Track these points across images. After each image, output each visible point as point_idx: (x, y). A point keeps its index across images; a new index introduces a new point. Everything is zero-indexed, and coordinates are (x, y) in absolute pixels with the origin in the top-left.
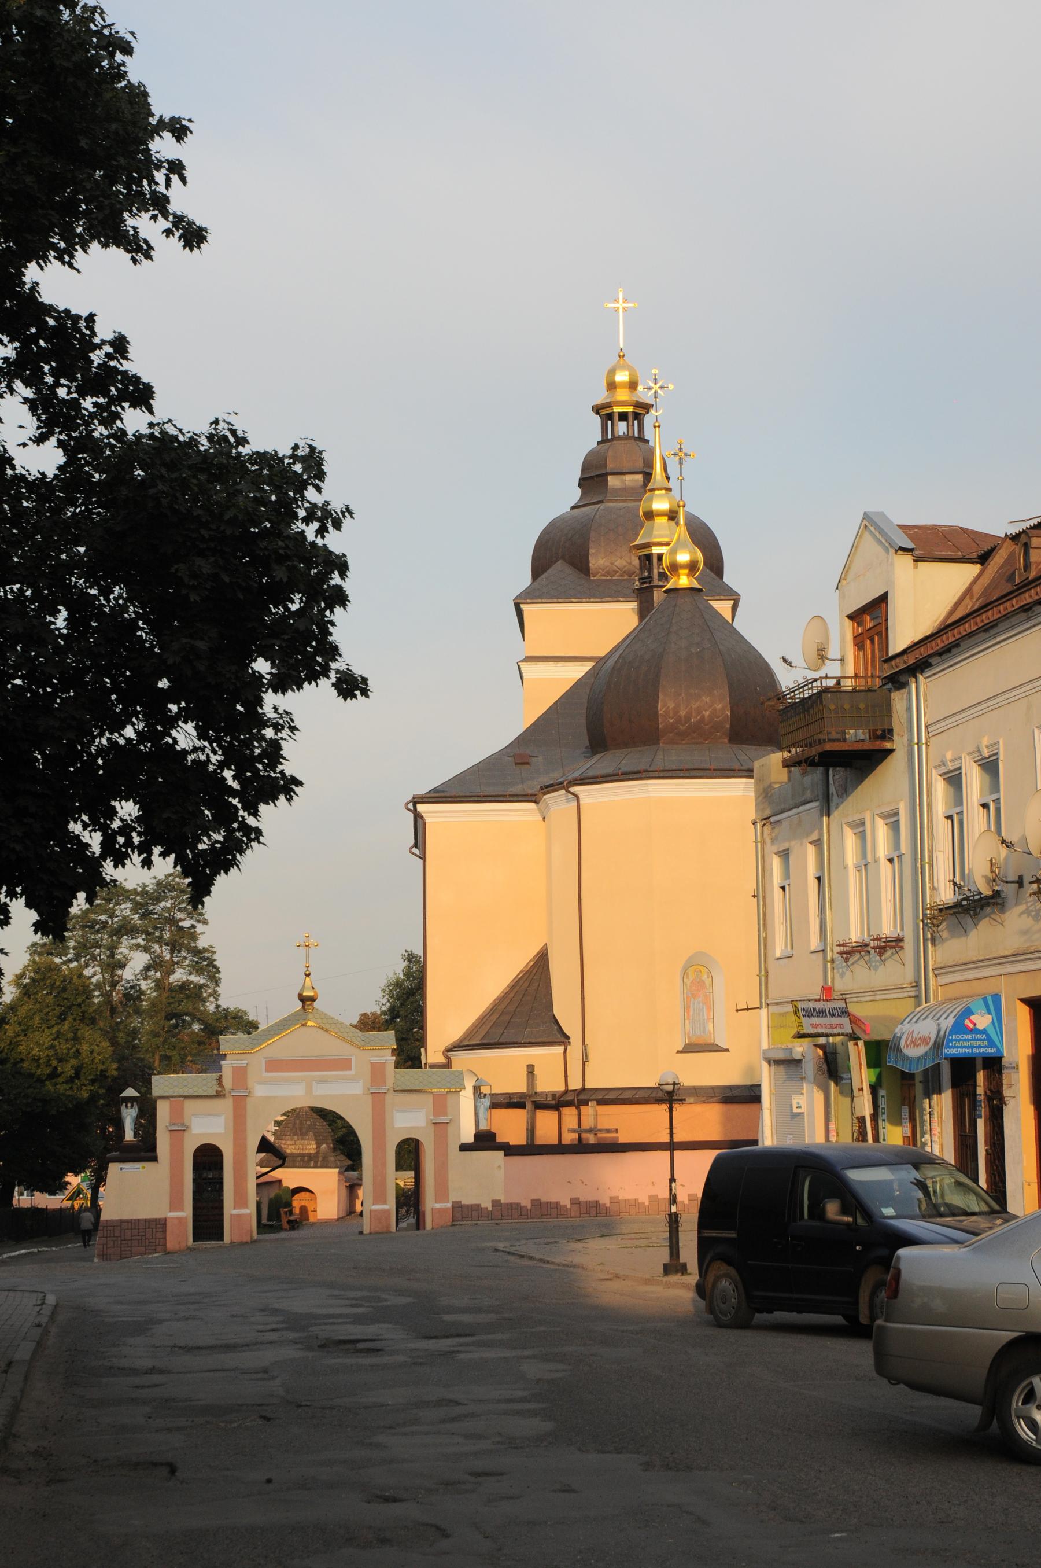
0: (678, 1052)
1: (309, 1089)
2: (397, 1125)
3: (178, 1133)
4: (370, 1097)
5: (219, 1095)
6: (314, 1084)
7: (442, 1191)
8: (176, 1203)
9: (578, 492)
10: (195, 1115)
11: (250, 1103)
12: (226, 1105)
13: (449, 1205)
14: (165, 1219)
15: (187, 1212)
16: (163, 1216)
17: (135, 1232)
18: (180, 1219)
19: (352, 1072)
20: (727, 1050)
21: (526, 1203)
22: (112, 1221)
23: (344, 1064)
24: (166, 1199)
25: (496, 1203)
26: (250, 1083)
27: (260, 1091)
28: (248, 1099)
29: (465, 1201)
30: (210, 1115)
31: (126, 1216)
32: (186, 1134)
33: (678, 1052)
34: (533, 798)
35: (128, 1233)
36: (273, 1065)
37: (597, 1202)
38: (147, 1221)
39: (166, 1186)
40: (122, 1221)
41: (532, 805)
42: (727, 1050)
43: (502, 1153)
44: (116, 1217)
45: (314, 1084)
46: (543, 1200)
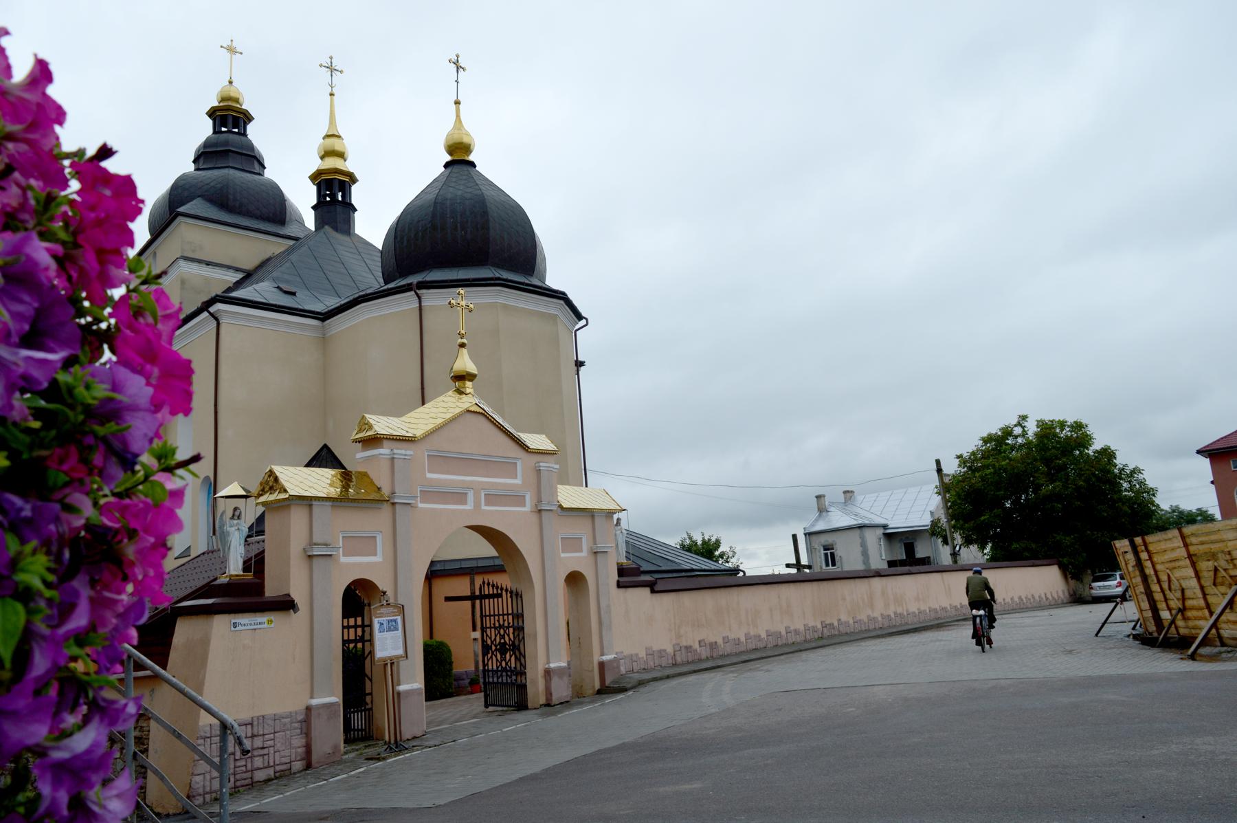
9: (191, 168)
23: (508, 467)
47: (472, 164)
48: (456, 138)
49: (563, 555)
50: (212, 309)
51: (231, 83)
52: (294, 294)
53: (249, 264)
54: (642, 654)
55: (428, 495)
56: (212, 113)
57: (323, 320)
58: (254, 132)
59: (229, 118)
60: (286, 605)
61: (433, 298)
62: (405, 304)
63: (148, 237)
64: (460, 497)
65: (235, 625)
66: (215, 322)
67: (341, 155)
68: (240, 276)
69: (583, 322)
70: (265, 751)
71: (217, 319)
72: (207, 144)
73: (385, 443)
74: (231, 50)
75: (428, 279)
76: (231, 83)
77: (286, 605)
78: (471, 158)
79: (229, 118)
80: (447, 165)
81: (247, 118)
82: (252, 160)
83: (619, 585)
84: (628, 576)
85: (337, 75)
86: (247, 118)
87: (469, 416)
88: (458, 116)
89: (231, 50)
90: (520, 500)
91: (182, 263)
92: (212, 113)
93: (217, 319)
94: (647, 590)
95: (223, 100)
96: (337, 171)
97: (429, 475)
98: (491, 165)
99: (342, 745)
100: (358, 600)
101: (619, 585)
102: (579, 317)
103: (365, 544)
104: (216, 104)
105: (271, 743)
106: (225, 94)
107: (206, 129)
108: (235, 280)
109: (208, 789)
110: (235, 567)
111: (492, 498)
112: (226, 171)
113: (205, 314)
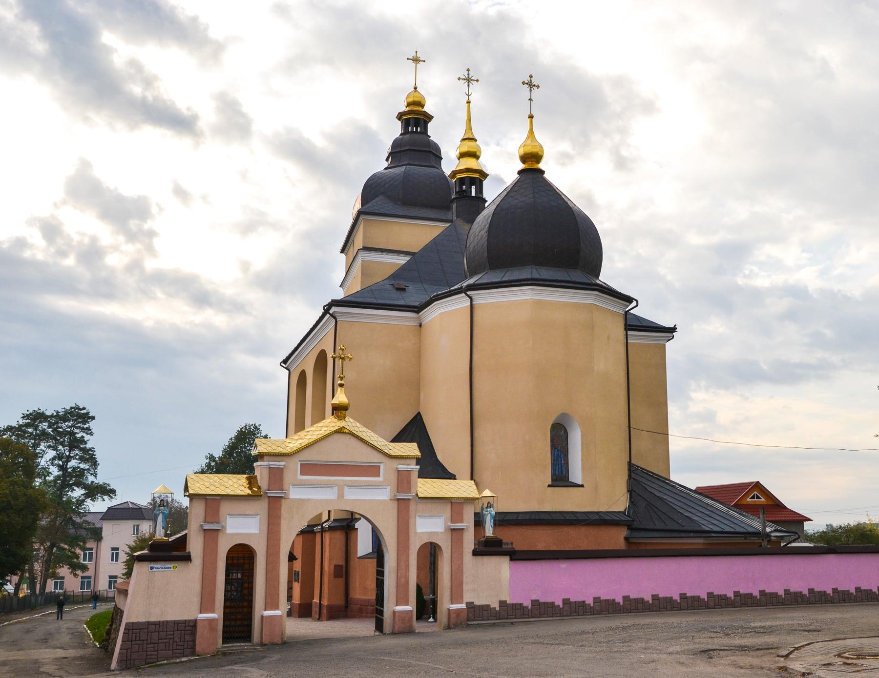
0: (549, 486)
1: (341, 495)
2: (419, 530)
3: (211, 535)
4: (396, 503)
5: (255, 496)
6: (346, 489)
7: (456, 594)
8: (206, 605)
10: (231, 515)
11: (284, 505)
12: (262, 506)
13: (464, 606)
14: (196, 621)
15: (217, 615)
16: (192, 618)
17: (163, 634)
18: (211, 621)
19: (380, 479)
20: (582, 486)
21: (527, 604)
22: (138, 623)
23: (373, 470)
24: (196, 600)
25: (502, 603)
26: (285, 486)
27: (294, 494)
28: (283, 501)
29: (477, 602)
30: (246, 515)
31: (153, 619)
32: (221, 535)
33: (549, 486)
35: (155, 636)
36: (308, 468)
38: (176, 623)
39: (197, 587)
40: (149, 623)
42: (582, 486)
44: (142, 619)
45: (346, 489)
46: (542, 600)
47: (543, 172)
48: (530, 149)
50: (331, 312)
51: (415, 88)
52: (404, 290)
56: (400, 116)
57: (418, 312)
58: (434, 131)
59: (415, 119)
62: (460, 303)
65: (152, 568)
66: (334, 320)
67: (475, 155)
68: (408, 258)
69: (634, 303)
71: (335, 318)
72: (396, 144)
73: (266, 458)
74: (416, 60)
76: (415, 88)
78: (541, 166)
79: (415, 119)
80: (519, 173)
81: (430, 118)
82: (433, 154)
83: (475, 553)
84: (487, 548)
85: (474, 85)
86: (430, 118)
87: (337, 436)
88: (531, 131)
89: (416, 60)
92: (400, 116)
93: (335, 318)
94: (507, 558)
95: (409, 105)
96: (468, 170)
98: (555, 173)
99: (220, 641)
101: (475, 553)
102: (629, 300)
104: (403, 108)
106: (411, 100)
107: (396, 130)
108: (404, 262)
113: (328, 315)
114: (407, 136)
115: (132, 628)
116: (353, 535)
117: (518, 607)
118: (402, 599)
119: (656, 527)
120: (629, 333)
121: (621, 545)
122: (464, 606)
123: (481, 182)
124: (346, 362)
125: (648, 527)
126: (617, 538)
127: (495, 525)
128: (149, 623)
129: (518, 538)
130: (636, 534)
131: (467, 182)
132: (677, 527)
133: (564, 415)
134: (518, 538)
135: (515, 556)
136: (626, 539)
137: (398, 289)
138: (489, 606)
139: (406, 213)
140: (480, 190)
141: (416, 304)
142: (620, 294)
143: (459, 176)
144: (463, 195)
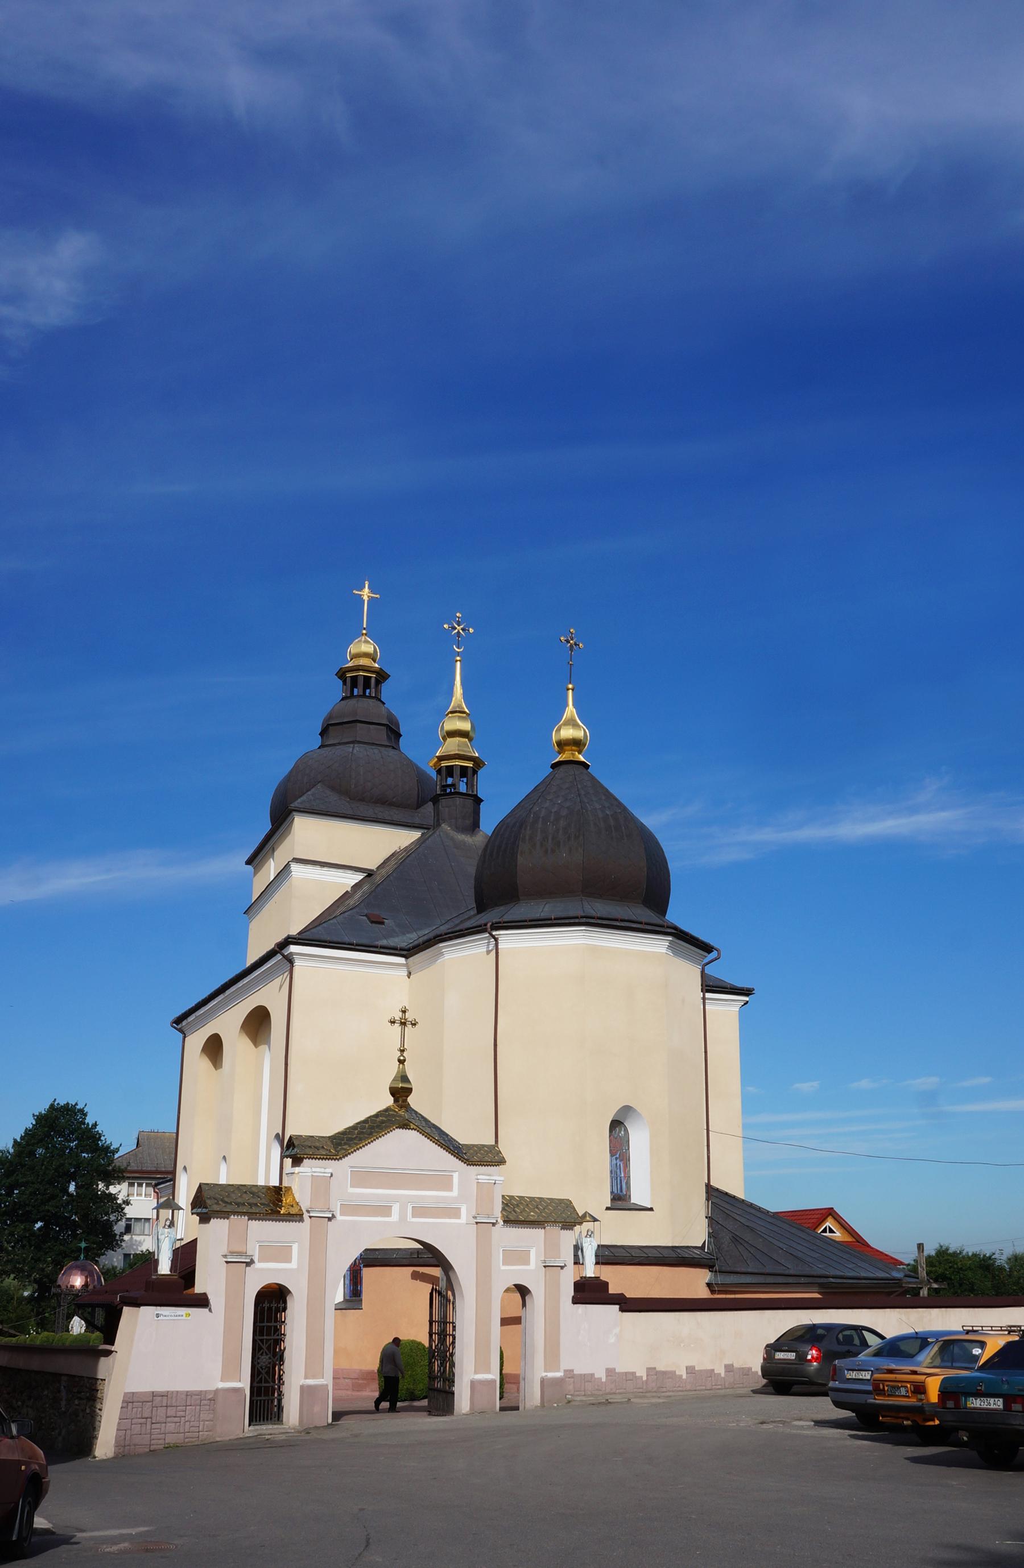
0: (608, 1209)
8: (229, 1371)
15: (244, 1383)
17: (171, 1412)
20: (651, 1209)
23: (443, 1182)
33: (608, 1209)
34: (408, 952)
37: (713, 1370)
38: (188, 1394)
41: (402, 960)
42: (651, 1209)
43: (617, 1307)
49: (503, 1268)
52: (383, 923)
53: (373, 866)
54: (642, 1373)
55: (350, 1209)
60: (202, 1302)
61: (511, 941)
63: (269, 827)
64: (384, 1210)
65: (158, 1316)
68: (359, 877)
69: (714, 954)
70: (176, 1419)
75: (506, 918)
77: (202, 1302)
84: (590, 1292)
90: (455, 1213)
91: (295, 867)
97: (351, 1190)
100: (272, 1302)
103: (282, 1253)
105: (182, 1413)
109: (127, 1443)
110: (164, 1267)
111: (420, 1211)
112: (349, 748)
113: (279, 957)
114: (352, 702)
115: (130, 1401)
116: (451, 1274)
117: (631, 1377)
118: (482, 1365)
119: (750, 1270)
120: (708, 995)
121: (704, 1293)
122: (559, 1374)
123: (475, 772)
124: (409, 1028)
125: (738, 1270)
126: (695, 1283)
127: (597, 1263)
128: (154, 1394)
129: (621, 1280)
130: (720, 1279)
131: (457, 772)
132: (779, 1270)
133: (627, 1110)
134: (621, 1280)
135: (628, 1305)
136: (709, 1285)
137: (372, 922)
138: (592, 1375)
139: (396, 818)
140: (470, 785)
141: (404, 945)
142: (697, 939)
143: (444, 764)
144: (448, 792)
